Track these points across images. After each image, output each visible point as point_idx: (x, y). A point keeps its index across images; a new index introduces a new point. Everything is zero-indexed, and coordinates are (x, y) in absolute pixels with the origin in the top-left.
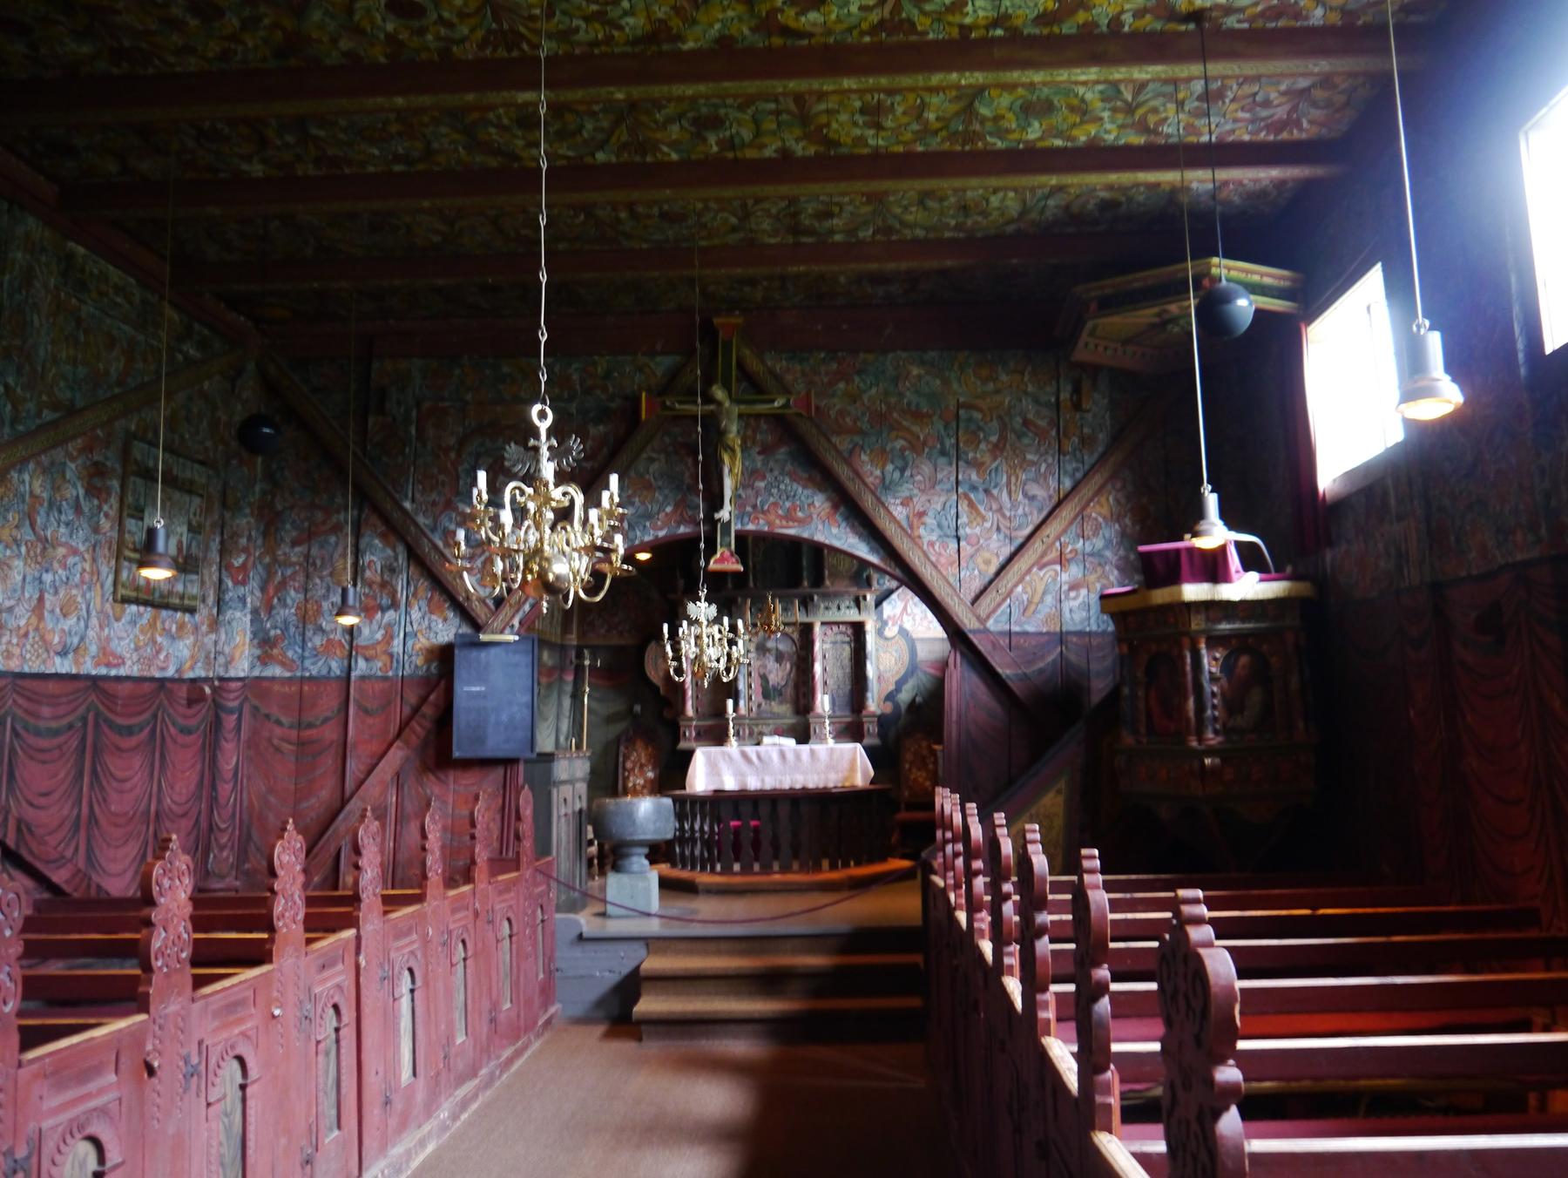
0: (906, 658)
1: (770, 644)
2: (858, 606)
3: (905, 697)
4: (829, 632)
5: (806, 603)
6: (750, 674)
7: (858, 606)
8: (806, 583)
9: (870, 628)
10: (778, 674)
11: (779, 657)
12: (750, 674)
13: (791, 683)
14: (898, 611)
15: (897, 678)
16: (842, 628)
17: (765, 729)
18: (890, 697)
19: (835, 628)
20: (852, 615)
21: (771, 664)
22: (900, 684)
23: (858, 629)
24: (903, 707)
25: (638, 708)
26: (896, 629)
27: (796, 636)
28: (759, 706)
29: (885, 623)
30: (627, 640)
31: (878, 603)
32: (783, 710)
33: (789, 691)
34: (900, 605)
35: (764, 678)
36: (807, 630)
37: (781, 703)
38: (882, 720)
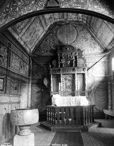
0: (93, 81)
1: (67, 78)
2: (84, 70)
3: (92, 88)
4: (78, 76)
5: (74, 70)
6: (63, 84)
7: (84, 70)
8: (74, 66)
9: (86, 74)
10: (69, 84)
11: (69, 80)
12: (63, 84)
13: (71, 85)
14: (91, 72)
15: (91, 84)
16: (81, 75)
17: (66, 94)
18: (90, 88)
19: (79, 75)
20: (83, 72)
21: (67, 81)
22: (92, 85)
23: (84, 75)
24: (92, 90)
25: (43, 90)
26: (91, 75)
27: (72, 76)
28: (65, 89)
29: (89, 74)
30: (41, 78)
31: (88, 70)
32: (70, 90)
33: (71, 87)
34: (92, 70)
35: (66, 84)
36: (74, 75)
37: (69, 89)
38: (89, 93)
